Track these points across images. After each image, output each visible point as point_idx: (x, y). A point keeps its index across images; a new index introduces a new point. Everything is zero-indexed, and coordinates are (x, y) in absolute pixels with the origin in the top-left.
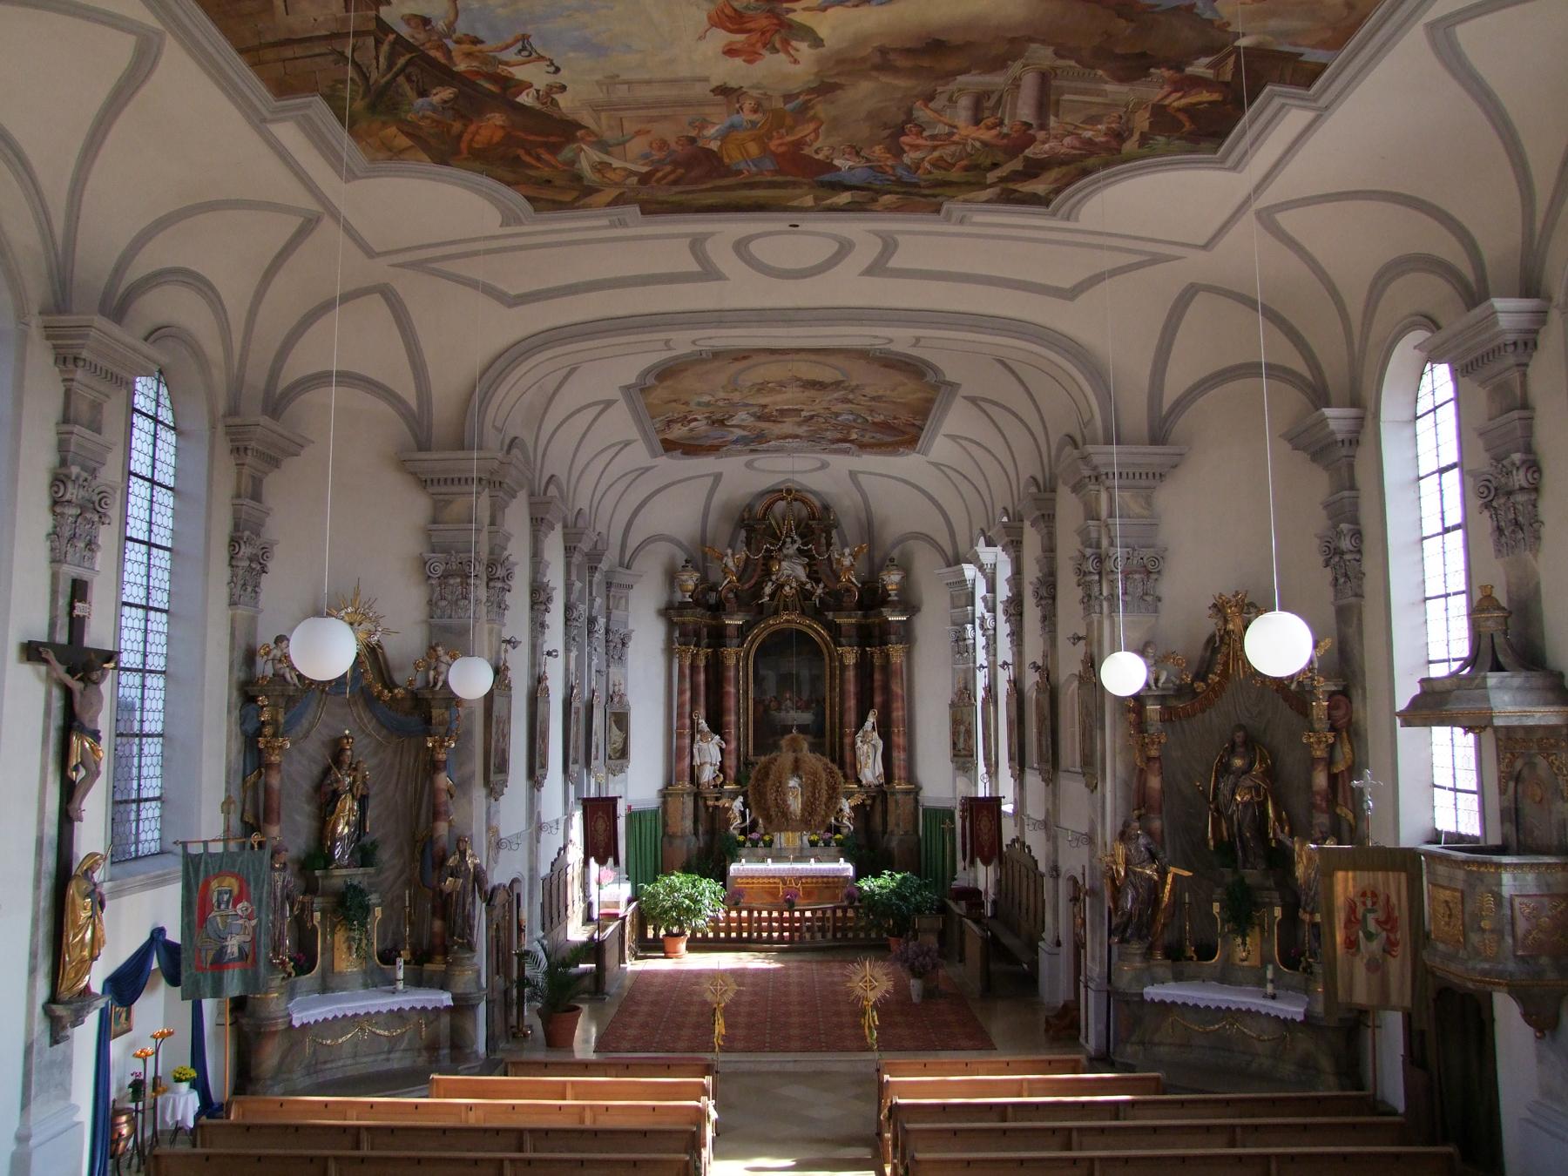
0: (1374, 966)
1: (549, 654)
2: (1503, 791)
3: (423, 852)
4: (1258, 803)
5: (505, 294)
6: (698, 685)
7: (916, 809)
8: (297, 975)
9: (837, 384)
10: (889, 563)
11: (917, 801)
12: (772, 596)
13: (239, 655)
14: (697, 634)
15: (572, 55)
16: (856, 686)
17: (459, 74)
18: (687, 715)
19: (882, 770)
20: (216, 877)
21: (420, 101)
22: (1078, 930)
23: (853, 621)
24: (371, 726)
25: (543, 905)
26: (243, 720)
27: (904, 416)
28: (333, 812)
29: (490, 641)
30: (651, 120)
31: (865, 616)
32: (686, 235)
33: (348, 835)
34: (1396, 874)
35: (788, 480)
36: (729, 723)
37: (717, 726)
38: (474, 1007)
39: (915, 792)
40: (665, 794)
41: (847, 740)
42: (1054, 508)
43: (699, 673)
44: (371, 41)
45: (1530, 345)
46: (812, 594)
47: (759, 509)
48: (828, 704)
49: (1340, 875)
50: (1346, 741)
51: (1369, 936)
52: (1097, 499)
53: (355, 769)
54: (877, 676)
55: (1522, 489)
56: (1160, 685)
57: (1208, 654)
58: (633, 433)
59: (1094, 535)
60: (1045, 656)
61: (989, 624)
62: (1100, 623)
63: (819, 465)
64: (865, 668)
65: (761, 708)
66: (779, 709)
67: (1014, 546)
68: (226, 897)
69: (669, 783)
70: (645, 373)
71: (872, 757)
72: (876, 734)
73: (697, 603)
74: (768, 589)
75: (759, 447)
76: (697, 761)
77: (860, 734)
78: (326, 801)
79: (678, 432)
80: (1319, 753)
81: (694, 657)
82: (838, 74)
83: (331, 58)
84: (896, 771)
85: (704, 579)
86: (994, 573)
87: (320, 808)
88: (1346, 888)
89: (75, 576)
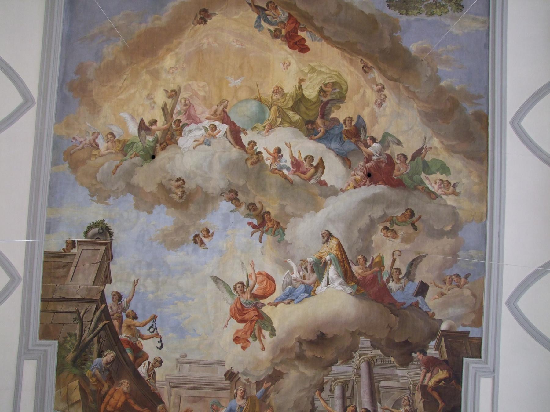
15: (171, 335)
17: (119, 339)
21: (97, 360)
30: (196, 400)
44: (94, 306)
82: (281, 363)
83: (75, 316)
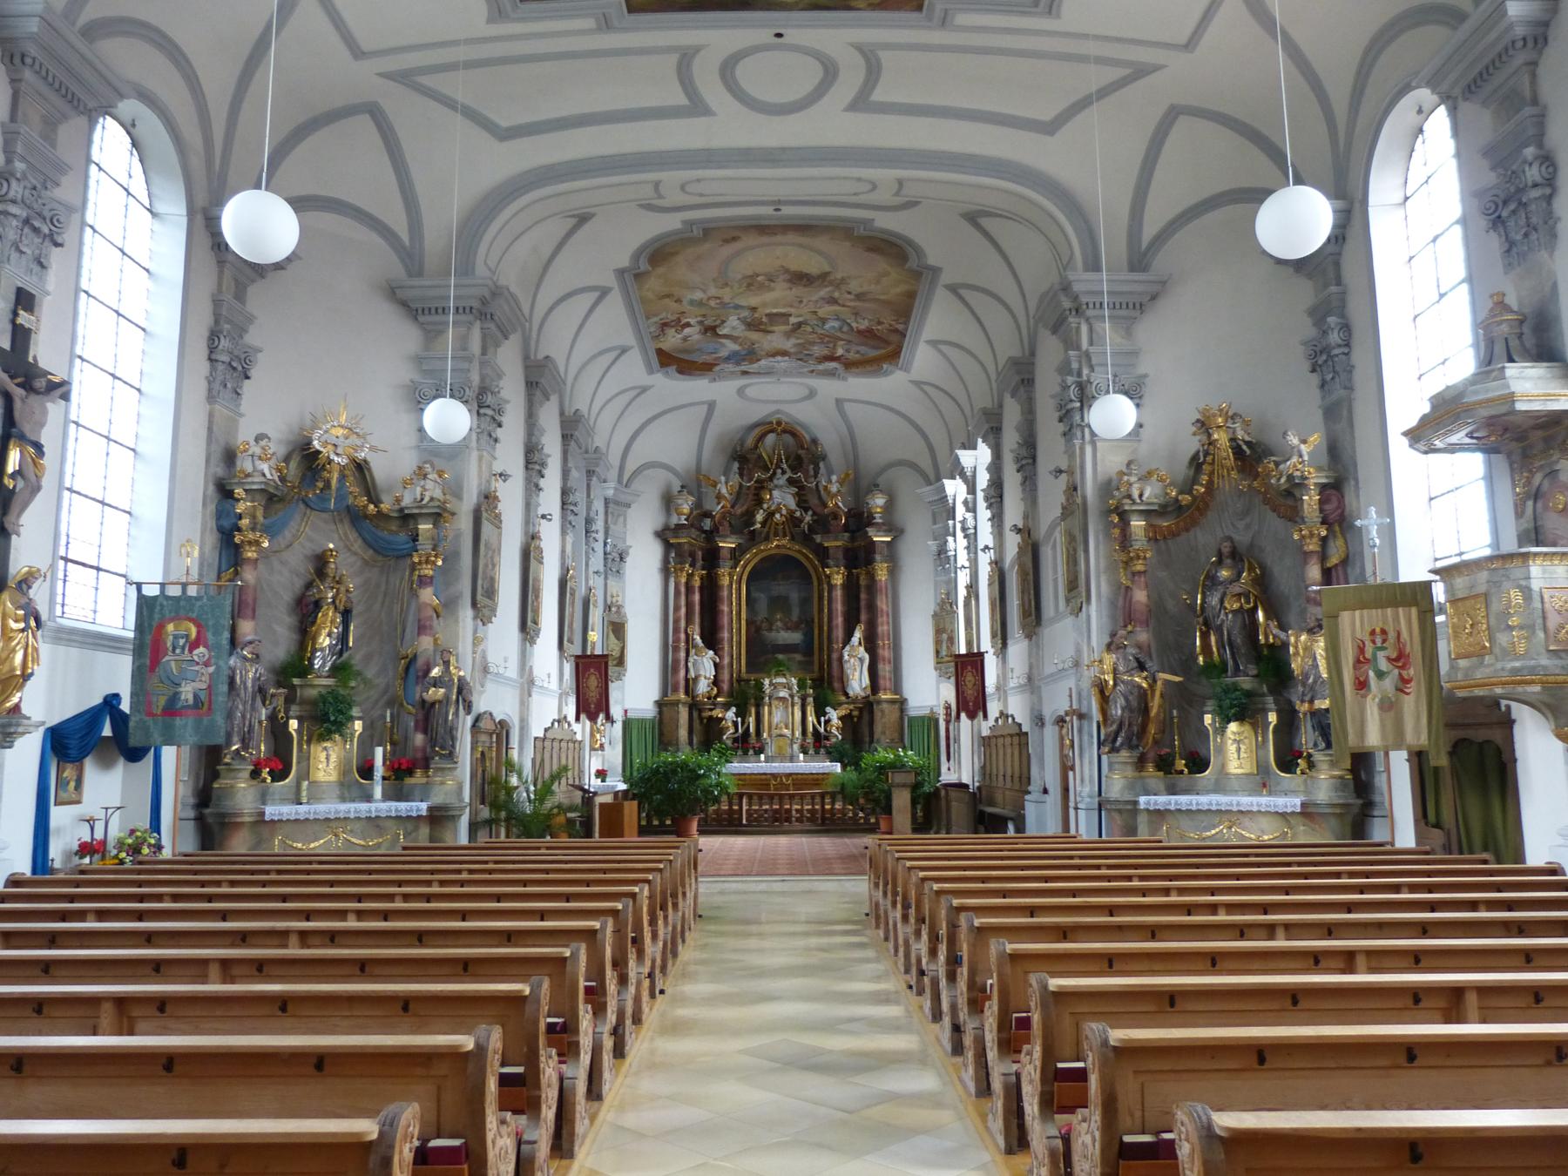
0: (1387, 706)
1: (543, 517)
2: (1519, 514)
3: (407, 669)
4: (1248, 611)
5: (497, 126)
7: (902, 718)
8: (273, 780)
9: (823, 277)
10: (874, 487)
12: (764, 524)
13: (217, 451)
14: (692, 555)
16: (844, 604)
18: (682, 630)
20: (171, 620)
22: (1066, 752)
24: (358, 545)
25: (534, 760)
26: (220, 515)
27: (888, 320)
28: (314, 623)
29: (480, 467)
31: (853, 539)
32: (670, 50)
33: (330, 646)
34: (1407, 609)
35: (778, 412)
36: (723, 639)
37: (711, 641)
38: (455, 819)
39: (902, 703)
40: (660, 704)
41: (835, 656)
42: (1032, 372)
45: (1540, 41)
46: (801, 521)
47: (750, 442)
48: (816, 625)
49: (1345, 616)
50: (1339, 535)
51: (1380, 675)
52: (1078, 329)
53: (338, 583)
54: (863, 596)
55: (1535, 185)
56: (1144, 498)
57: (1192, 472)
58: (629, 338)
59: (1075, 366)
60: (1026, 517)
61: (970, 523)
62: (1082, 449)
63: (806, 392)
64: (851, 588)
65: (753, 629)
66: (770, 630)
67: (994, 434)
68: (182, 642)
69: (664, 692)
70: (636, 256)
71: (858, 669)
72: (862, 649)
73: (692, 525)
74: (759, 517)
75: (754, 367)
76: (692, 674)
77: (847, 648)
78: (306, 612)
79: (672, 340)
80: (1312, 546)
81: (690, 576)
84: (881, 682)
85: (698, 504)
86: (974, 476)
87: (301, 622)
88: (1353, 631)
89: (20, 285)
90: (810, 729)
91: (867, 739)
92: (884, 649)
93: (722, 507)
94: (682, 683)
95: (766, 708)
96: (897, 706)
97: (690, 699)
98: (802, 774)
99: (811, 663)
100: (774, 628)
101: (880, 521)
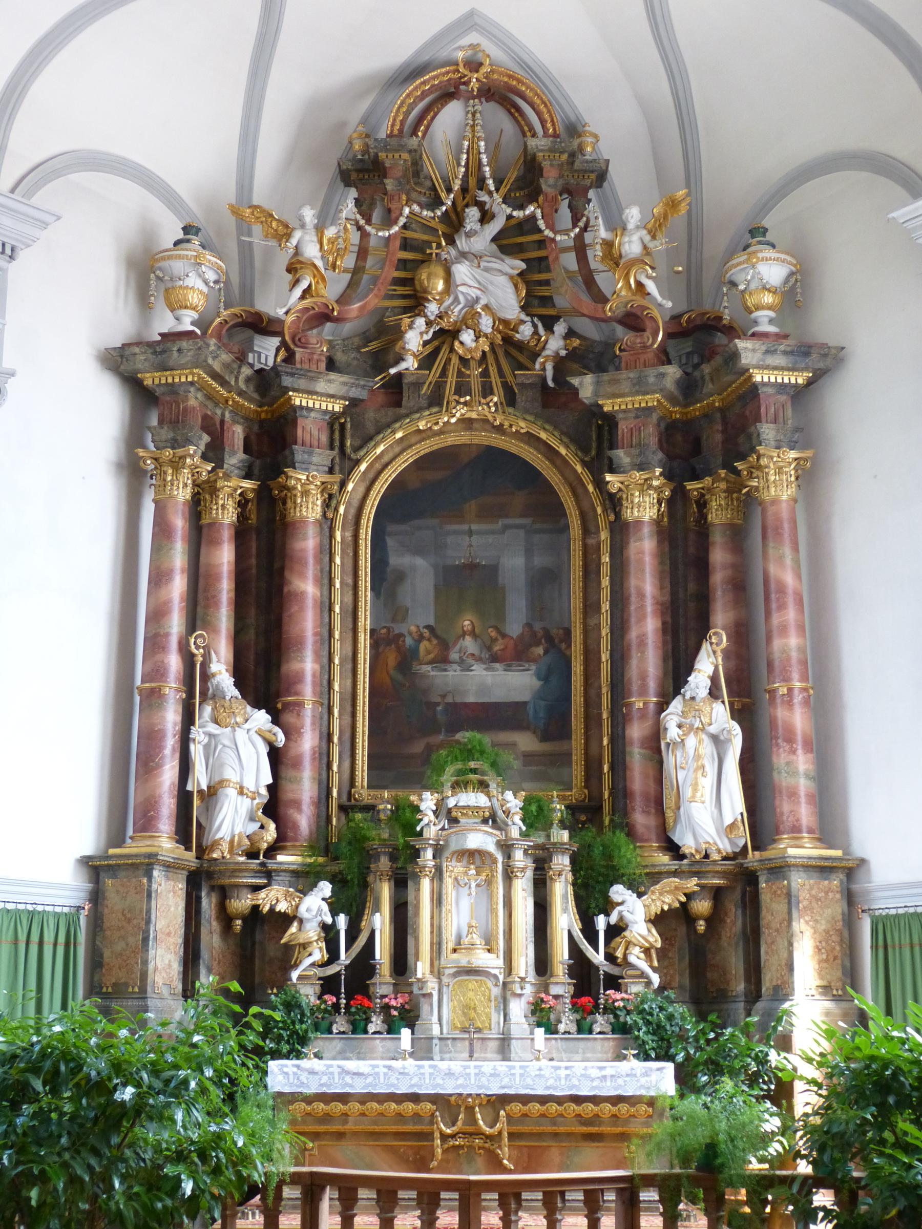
6: (213, 578)
11: (850, 898)
12: (427, 362)
16: (660, 576)
19: (739, 805)
23: (652, 400)
36: (299, 678)
41: (636, 731)
43: (215, 542)
54: (719, 556)
65: (392, 659)
66: (442, 660)
69: (116, 835)
76: (200, 778)
77: (676, 705)
90: (561, 952)
91: (740, 987)
92: (790, 704)
93: (306, 293)
94: (168, 806)
95: (426, 884)
96: (836, 882)
97: (191, 856)
98: (543, 1100)
99: (565, 759)
100: (454, 655)
101: (772, 329)
